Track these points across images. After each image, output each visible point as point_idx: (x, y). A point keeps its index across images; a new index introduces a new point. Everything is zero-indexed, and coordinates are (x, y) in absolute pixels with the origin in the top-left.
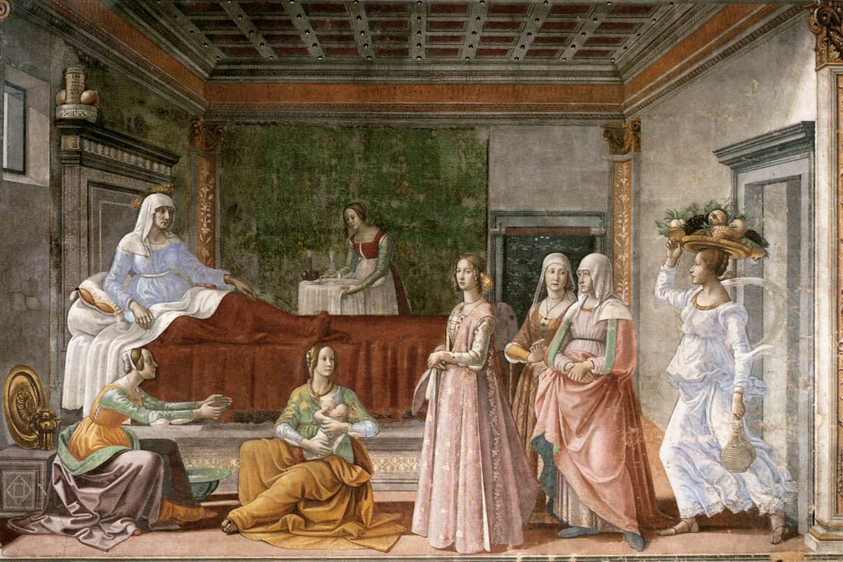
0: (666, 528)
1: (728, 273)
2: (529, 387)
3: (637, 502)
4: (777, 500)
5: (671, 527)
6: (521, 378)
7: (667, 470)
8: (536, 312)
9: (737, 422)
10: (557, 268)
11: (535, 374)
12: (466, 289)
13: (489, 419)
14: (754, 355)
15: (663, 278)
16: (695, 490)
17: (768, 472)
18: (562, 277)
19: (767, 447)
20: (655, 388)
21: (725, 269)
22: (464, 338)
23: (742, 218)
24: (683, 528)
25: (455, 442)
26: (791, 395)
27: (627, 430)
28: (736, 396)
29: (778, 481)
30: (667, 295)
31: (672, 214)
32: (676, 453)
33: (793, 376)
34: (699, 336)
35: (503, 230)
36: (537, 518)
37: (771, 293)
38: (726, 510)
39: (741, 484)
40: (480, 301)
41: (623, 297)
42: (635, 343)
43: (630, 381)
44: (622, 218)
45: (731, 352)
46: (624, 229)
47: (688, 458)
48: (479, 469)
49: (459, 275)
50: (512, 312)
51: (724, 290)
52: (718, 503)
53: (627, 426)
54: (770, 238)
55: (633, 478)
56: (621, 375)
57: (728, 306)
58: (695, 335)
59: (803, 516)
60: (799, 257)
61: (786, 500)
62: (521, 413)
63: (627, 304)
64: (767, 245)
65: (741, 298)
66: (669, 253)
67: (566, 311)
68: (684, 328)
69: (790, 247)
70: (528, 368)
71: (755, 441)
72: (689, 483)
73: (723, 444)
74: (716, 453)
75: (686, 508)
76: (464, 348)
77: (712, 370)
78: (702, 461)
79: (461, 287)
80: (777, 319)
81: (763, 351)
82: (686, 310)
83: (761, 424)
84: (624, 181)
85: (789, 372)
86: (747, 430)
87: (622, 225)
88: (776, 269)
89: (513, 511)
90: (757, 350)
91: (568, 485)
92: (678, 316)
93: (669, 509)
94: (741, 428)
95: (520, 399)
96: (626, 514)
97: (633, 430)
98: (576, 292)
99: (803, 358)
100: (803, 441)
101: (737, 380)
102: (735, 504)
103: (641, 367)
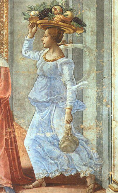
0: (28, 184)
1: (63, 41)
3: (11, 170)
4: (90, 169)
5: (30, 183)
7: (28, 151)
9: (68, 125)
14: (78, 87)
15: (26, 44)
16: (44, 163)
17: (85, 153)
19: (85, 139)
20: (21, 106)
21: (62, 39)
23: (71, 10)
24: (37, 184)
26: (99, 110)
27: (6, 129)
28: (67, 111)
29: (91, 158)
30: (29, 53)
31: (31, 8)
32: (34, 143)
33: (99, 100)
34: (47, 76)
37: (87, 53)
38: (62, 175)
39: (70, 160)
41: (4, 55)
43: (8, 101)
44: (3, 10)
45: (65, 85)
47: (40, 145)
51: (61, 51)
52: (57, 170)
53: (6, 127)
54: (87, 22)
55: (9, 156)
56: (3, 98)
57: (63, 60)
58: (44, 76)
59: (105, 177)
60: (103, 32)
61: (95, 169)
63: (6, 58)
64: (85, 25)
65: (70, 55)
66: (30, 30)
68: (38, 72)
69: (98, 26)
71: (78, 135)
72: (41, 160)
73: (60, 138)
74: (56, 143)
75: (39, 173)
77: (54, 96)
78: (48, 147)
80: (90, 67)
81: (83, 85)
82: (39, 62)
83: (82, 127)
85: (97, 98)
86: (73, 129)
87: (3, 14)
88: (89, 38)
90: (80, 84)
92: (35, 65)
93: (29, 173)
94: (71, 129)
97: (9, 130)
99: (106, 89)
100: (105, 136)
101: (68, 102)
102: (67, 171)
103: (14, 94)
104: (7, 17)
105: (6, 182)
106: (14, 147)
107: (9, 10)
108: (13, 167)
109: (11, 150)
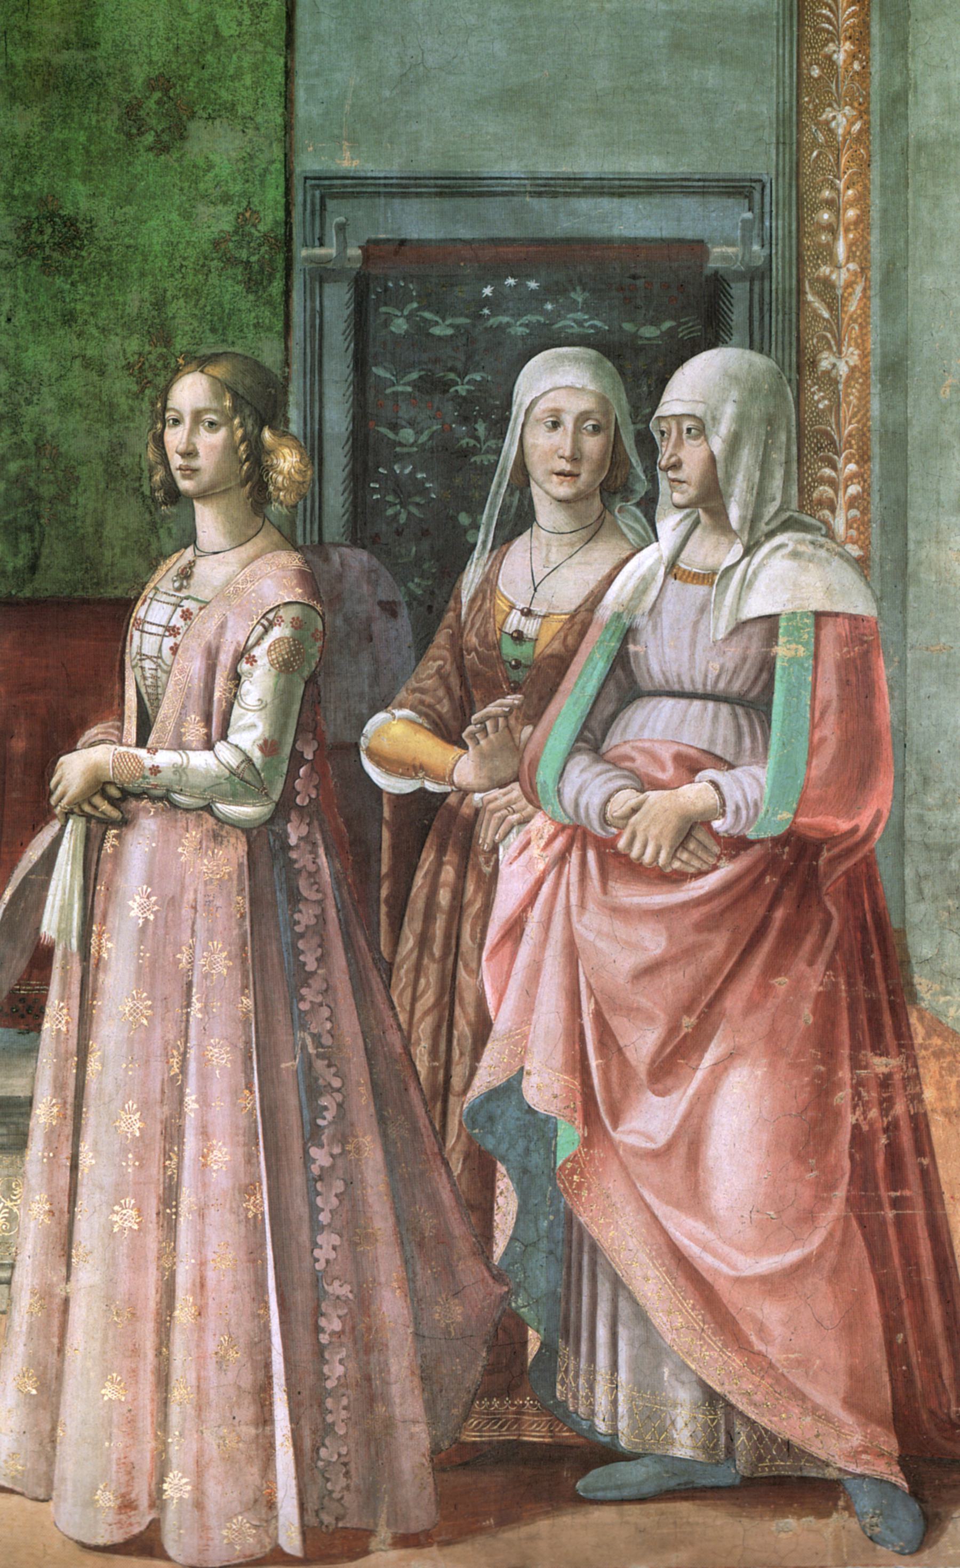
2: (458, 892)
3: (894, 1353)
6: (428, 858)
8: (488, 585)
10: (573, 406)
11: (486, 835)
12: (204, 495)
13: (300, 1021)
18: (592, 445)
22: (197, 684)
25: (162, 1112)
27: (856, 1064)
35: (354, 252)
36: (493, 1418)
40: (259, 542)
41: (839, 524)
42: (886, 711)
43: (869, 863)
44: (830, 204)
46: (841, 250)
48: (255, 1225)
49: (175, 438)
50: (388, 590)
53: (856, 1047)
55: (878, 1258)
56: (831, 839)
62: (428, 999)
63: (854, 551)
67: (610, 580)
70: (454, 812)
76: (194, 730)
79: (185, 485)
84: (841, 52)
87: (832, 230)
89: (395, 1390)
91: (617, 1284)
95: (424, 941)
96: (852, 1403)
97: (880, 1065)
98: (649, 505)
103: (912, 810)
104: (859, 251)
105: (857, 1440)
106: (913, 1191)
107: (876, 200)
108: (907, 1336)
109: (890, 1214)
